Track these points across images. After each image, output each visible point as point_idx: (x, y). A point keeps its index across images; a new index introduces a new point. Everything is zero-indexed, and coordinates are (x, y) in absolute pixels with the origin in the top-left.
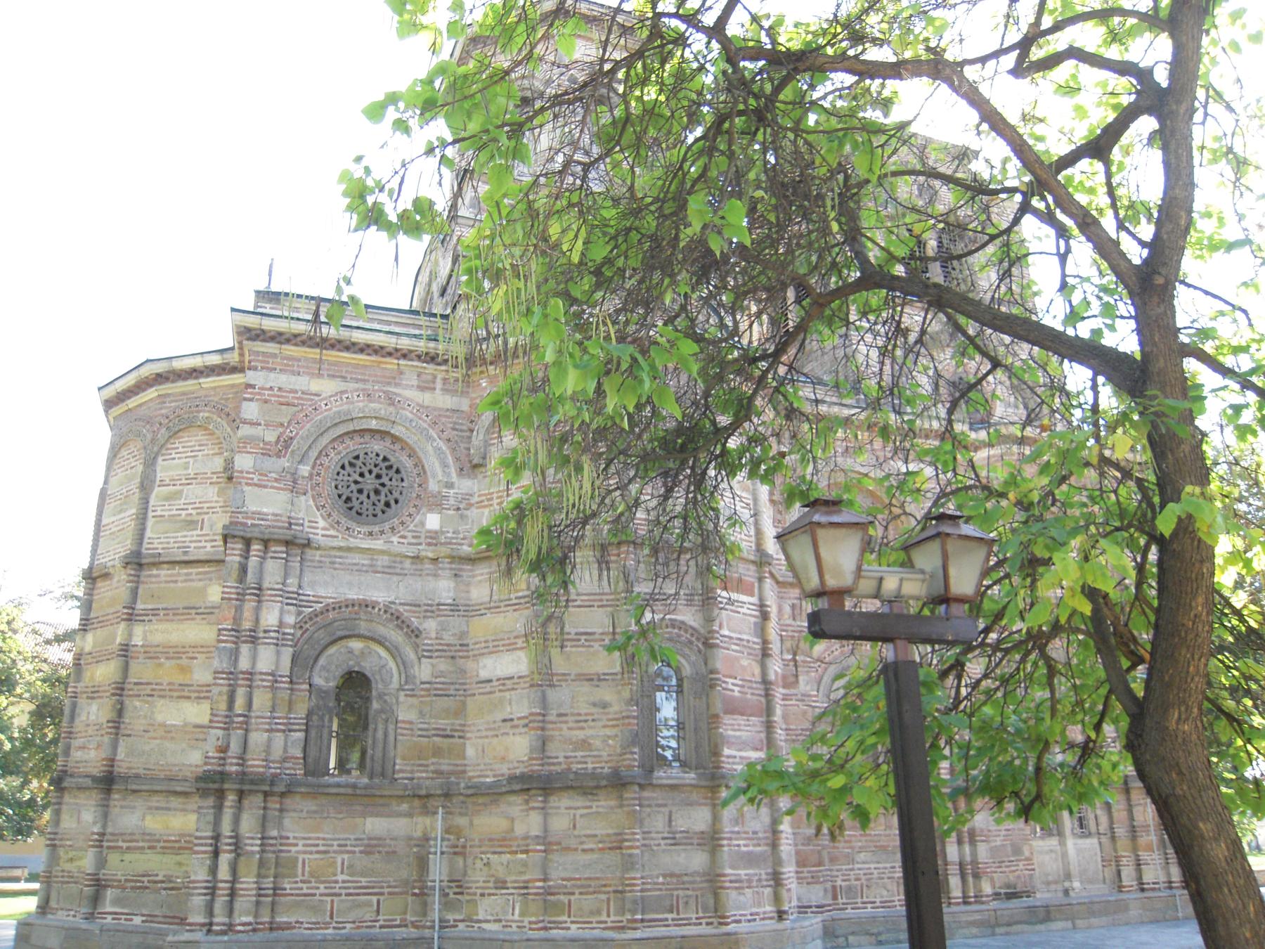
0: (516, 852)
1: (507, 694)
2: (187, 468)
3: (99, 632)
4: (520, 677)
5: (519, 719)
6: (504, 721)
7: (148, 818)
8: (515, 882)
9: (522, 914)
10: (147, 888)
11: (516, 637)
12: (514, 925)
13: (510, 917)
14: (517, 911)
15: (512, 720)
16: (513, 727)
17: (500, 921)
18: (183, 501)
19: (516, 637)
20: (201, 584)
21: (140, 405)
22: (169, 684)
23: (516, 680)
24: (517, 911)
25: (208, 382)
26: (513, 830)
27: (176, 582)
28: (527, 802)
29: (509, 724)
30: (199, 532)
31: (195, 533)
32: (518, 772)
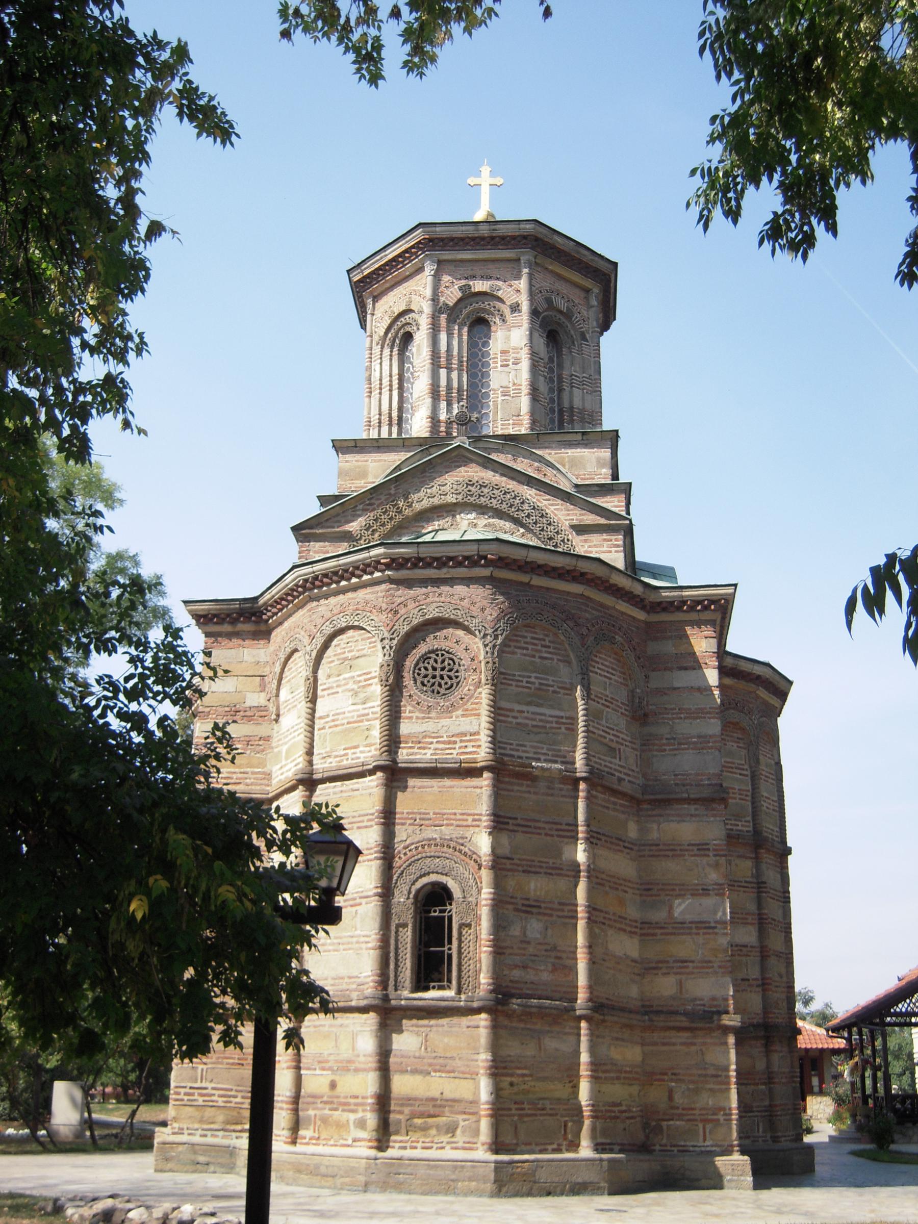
0: (757, 1084)
1: (744, 959)
2: (605, 689)
3: (520, 837)
4: (751, 947)
5: (753, 979)
6: (743, 980)
7: (613, 1048)
8: (758, 1107)
9: (764, 1131)
10: (618, 1118)
11: (747, 914)
12: (760, 1140)
13: (756, 1134)
14: (761, 1130)
15: (748, 980)
16: (750, 986)
17: (748, 1137)
18: (604, 722)
19: (747, 914)
20: (623, 817)
21: (548, 589)
22: (614, 914)
23: (749, 949)
24: (761, 1130)
25: (623, 607)
26: (754, 1067)
27: (608, 808)
28: (766, 1045)
29: (747, 983)
30: (617, 761)
31: (613, 760)
32: (755, 1021)
